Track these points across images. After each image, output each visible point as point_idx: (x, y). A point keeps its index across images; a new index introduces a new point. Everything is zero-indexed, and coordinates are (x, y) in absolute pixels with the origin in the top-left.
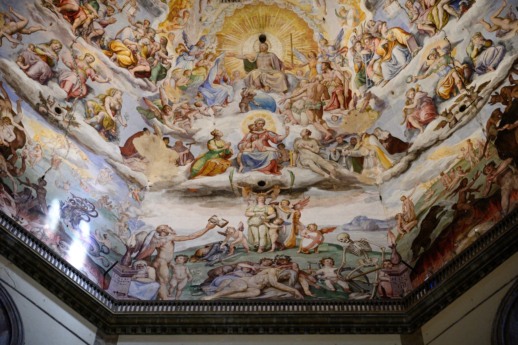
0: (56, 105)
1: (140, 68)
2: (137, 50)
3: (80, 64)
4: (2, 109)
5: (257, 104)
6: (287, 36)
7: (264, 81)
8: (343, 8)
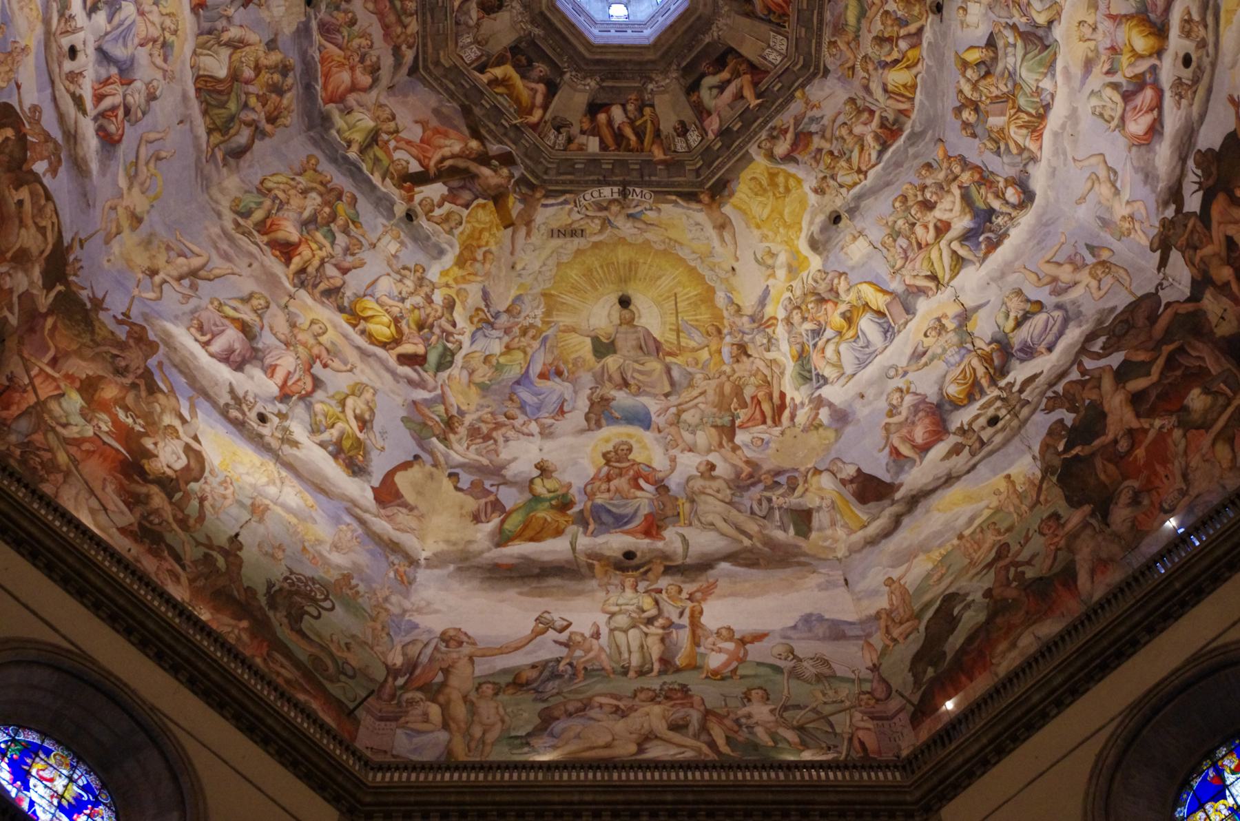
0: (259, 408)
1: (407, 348)
2: (402, 317)
3: (301, 336)
4: (163, 411)
5: (617, 415)
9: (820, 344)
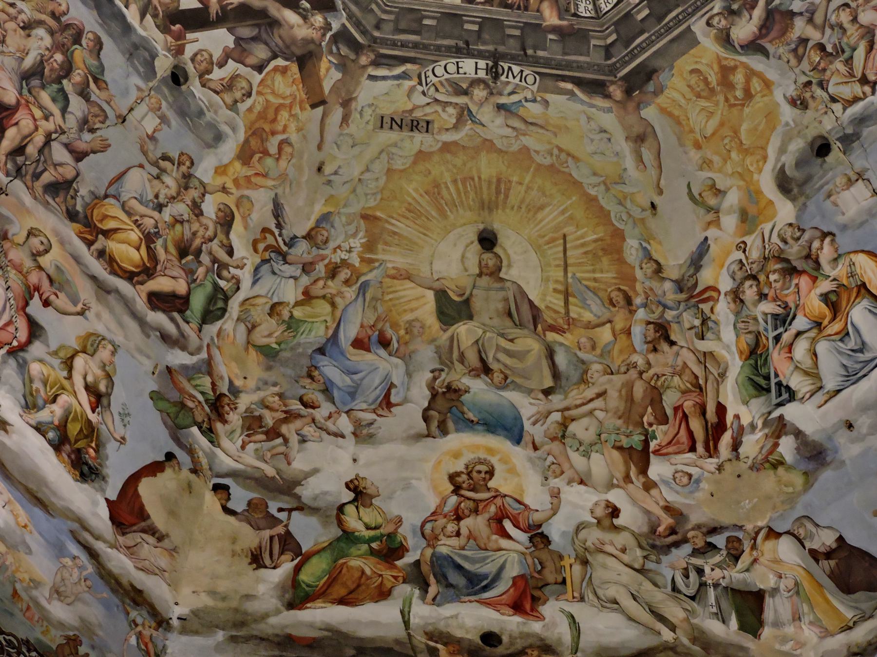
1: (161, 284)
2: (157, 234)
5: (471, 416)
6: (553, 240)
8: (710, 183)
9: (786, 337)
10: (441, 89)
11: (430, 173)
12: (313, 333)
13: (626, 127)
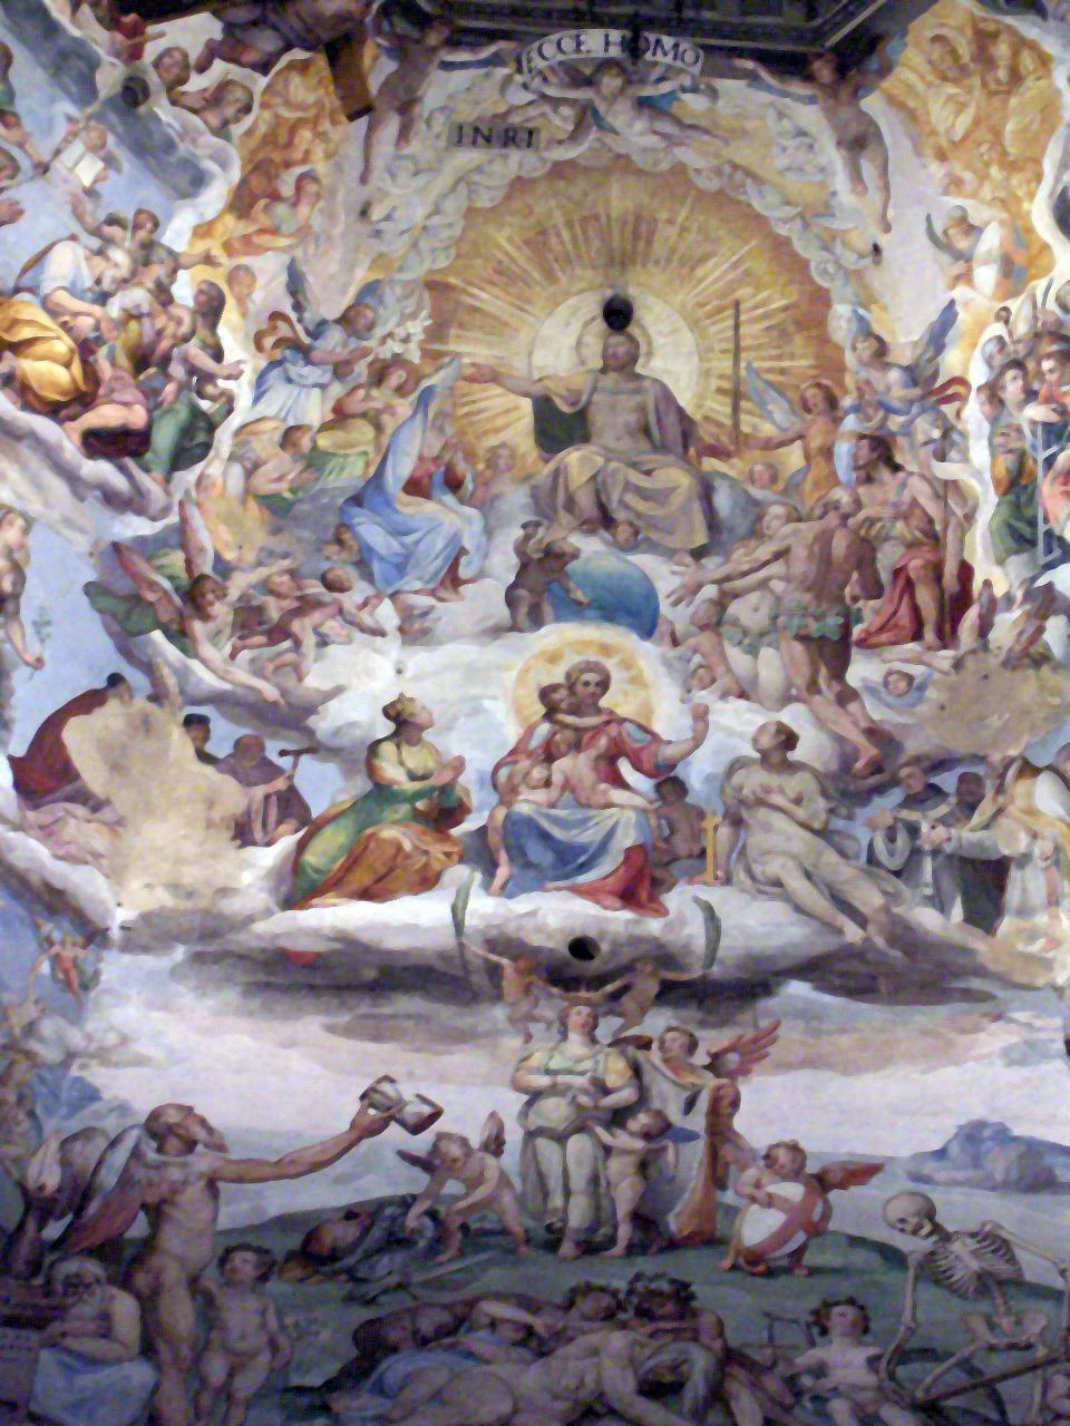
1: (107, 415)
5: (579, 595)
6: (721, 309)
7: (615, 497)
8: (958, 214)
10: (553, 79)
11: (531, 212)
12: (345, 474)
13: (838, 127)
